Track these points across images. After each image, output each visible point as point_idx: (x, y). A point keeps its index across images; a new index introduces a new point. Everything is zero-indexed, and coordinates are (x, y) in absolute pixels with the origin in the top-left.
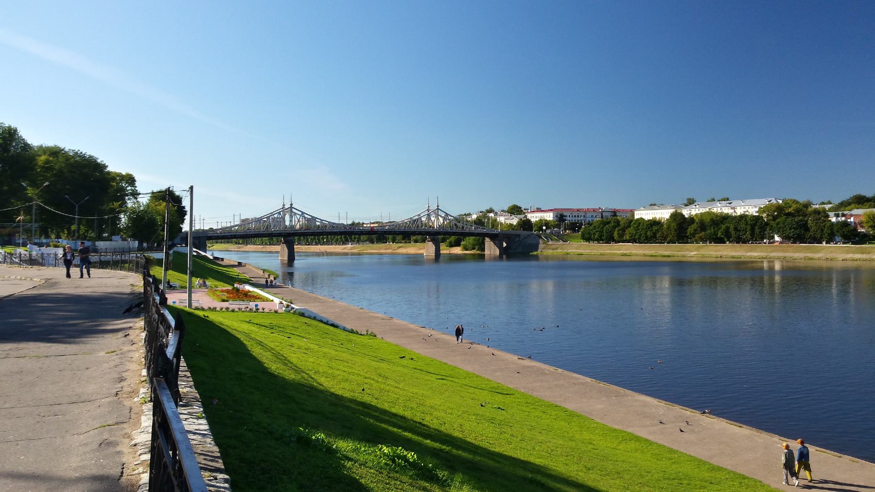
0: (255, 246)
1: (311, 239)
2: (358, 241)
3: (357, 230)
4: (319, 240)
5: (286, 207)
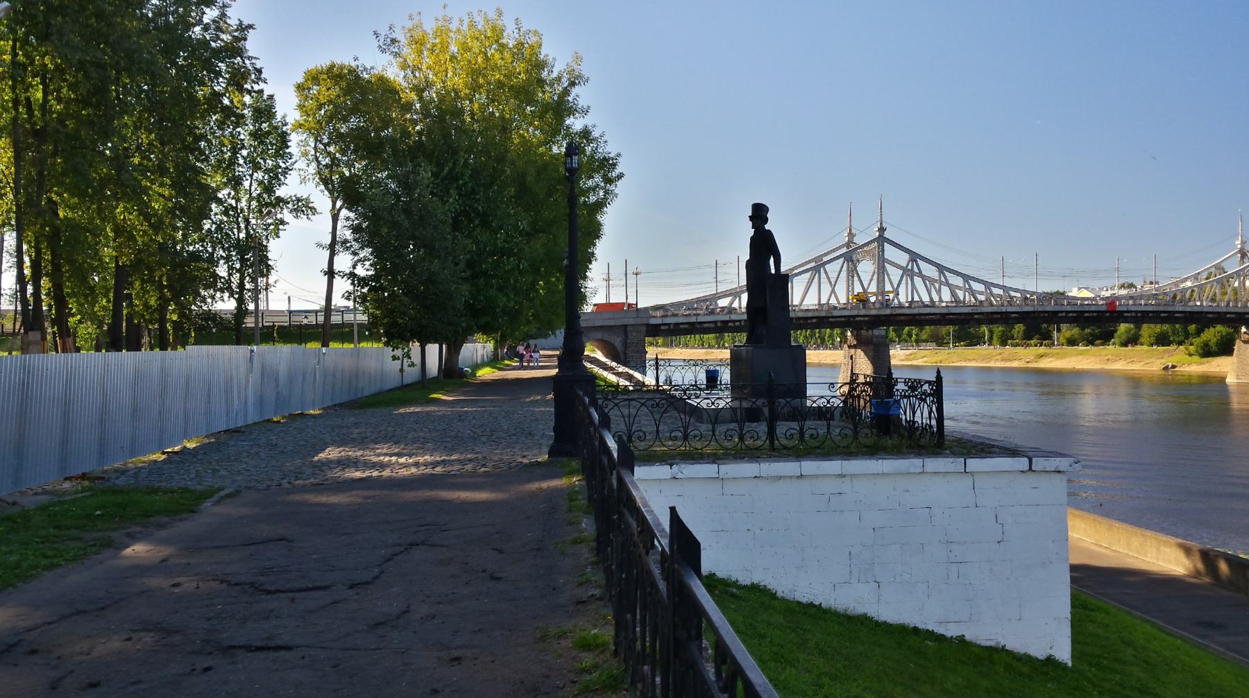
0: (689, 351)
1: (805, 337)
2: (917, 341)
3: (1069, 308)
4: (823, 340)
5: (860, 240)
